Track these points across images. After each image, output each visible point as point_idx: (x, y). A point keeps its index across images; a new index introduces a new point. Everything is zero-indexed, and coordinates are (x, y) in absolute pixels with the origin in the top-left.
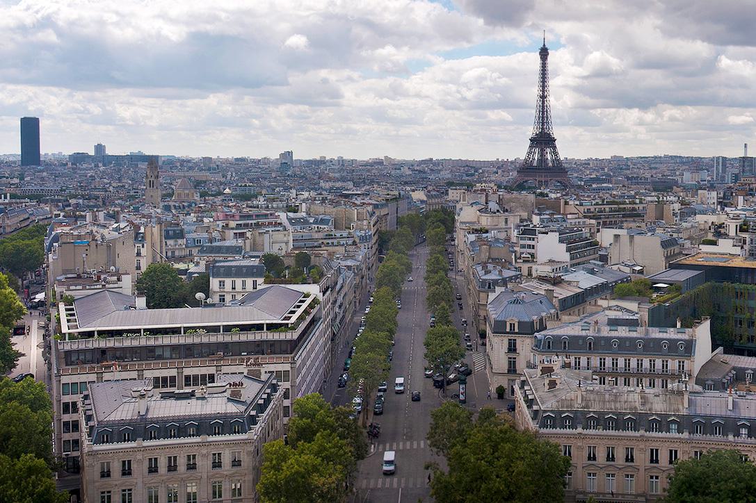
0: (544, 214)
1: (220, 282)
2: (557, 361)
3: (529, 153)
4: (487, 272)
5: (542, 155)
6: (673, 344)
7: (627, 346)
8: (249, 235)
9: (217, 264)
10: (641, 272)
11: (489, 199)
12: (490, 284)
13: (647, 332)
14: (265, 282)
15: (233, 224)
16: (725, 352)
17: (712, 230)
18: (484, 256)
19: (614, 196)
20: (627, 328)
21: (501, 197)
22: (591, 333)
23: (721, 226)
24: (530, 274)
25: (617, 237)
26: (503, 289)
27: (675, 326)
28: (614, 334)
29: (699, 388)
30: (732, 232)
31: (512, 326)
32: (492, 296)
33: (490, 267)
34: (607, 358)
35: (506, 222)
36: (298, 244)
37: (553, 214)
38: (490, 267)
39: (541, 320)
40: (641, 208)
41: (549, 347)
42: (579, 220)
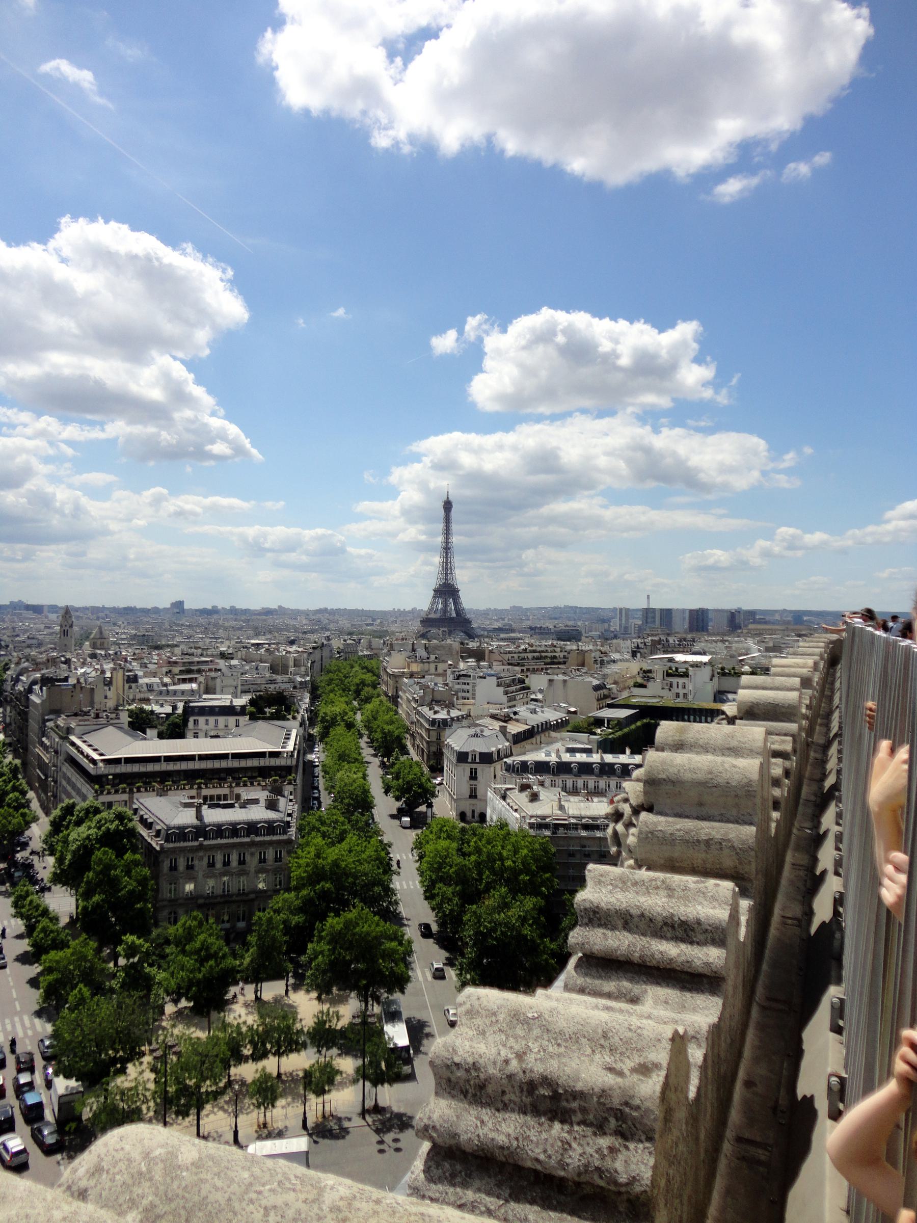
2: (532, 778)
3: (432, 604)
4: (435, 713)
5: (446, 605)
7: (585, 769)
9: (191, 704)
13: (602, 758)
14: (250, 719)
15: (176, 670)
18: (428, 699)
20: (584, 755)
22: (553, 758)
23: (650, 671)
25: (551, 681)
27: (624, 753)
31: (474, 757)
35: (436, 669)
38: (436, 708)
40: (562, 656)
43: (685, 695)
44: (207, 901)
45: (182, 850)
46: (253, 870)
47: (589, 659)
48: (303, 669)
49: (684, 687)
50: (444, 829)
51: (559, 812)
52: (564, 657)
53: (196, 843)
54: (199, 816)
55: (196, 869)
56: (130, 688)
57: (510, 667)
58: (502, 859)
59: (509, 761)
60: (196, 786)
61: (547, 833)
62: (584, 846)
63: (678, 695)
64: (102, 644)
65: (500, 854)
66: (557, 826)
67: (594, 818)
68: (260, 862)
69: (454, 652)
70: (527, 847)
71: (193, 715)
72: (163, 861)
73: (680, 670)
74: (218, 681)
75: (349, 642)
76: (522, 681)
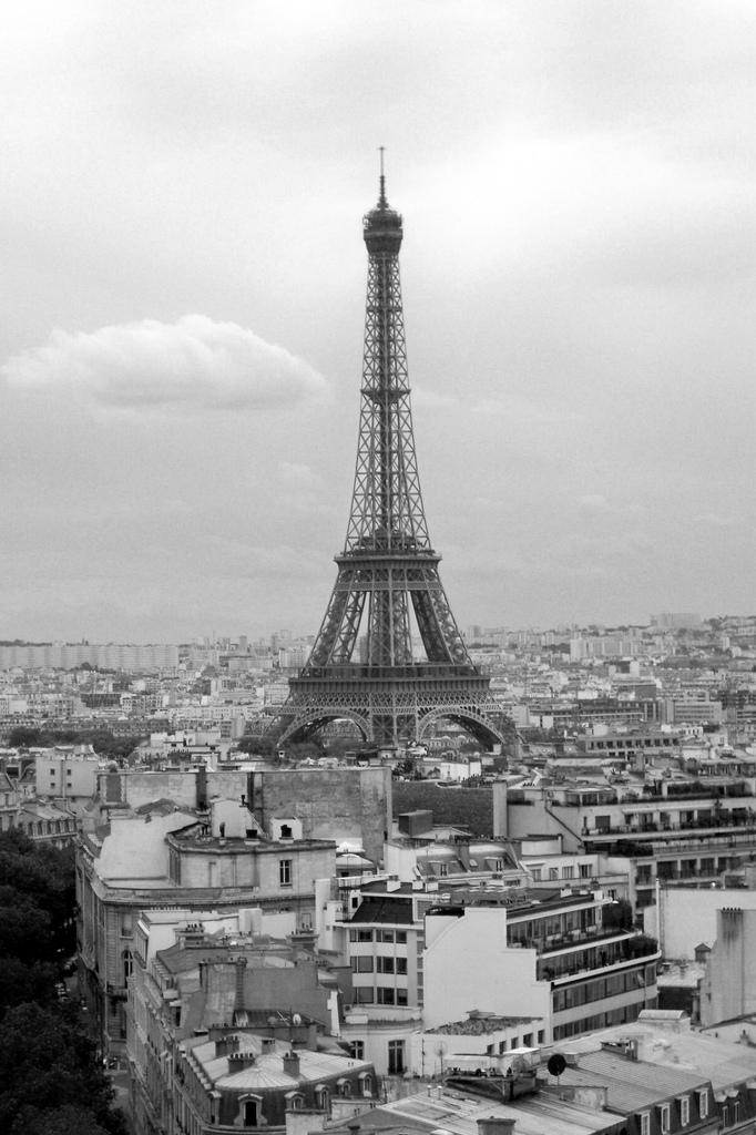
0: (426, 842)
3: (336, 613)
4: (239, 1064)
5: (385, 618)
11: (212, 788)
12: (251, 1107)
18: (221, 1005)
21: (258, 780)
25: (731, 917)
33: (249, 1044)
35: (286, 876)
57: (591, 859)
69: (370, 806)
76: (619, 917)
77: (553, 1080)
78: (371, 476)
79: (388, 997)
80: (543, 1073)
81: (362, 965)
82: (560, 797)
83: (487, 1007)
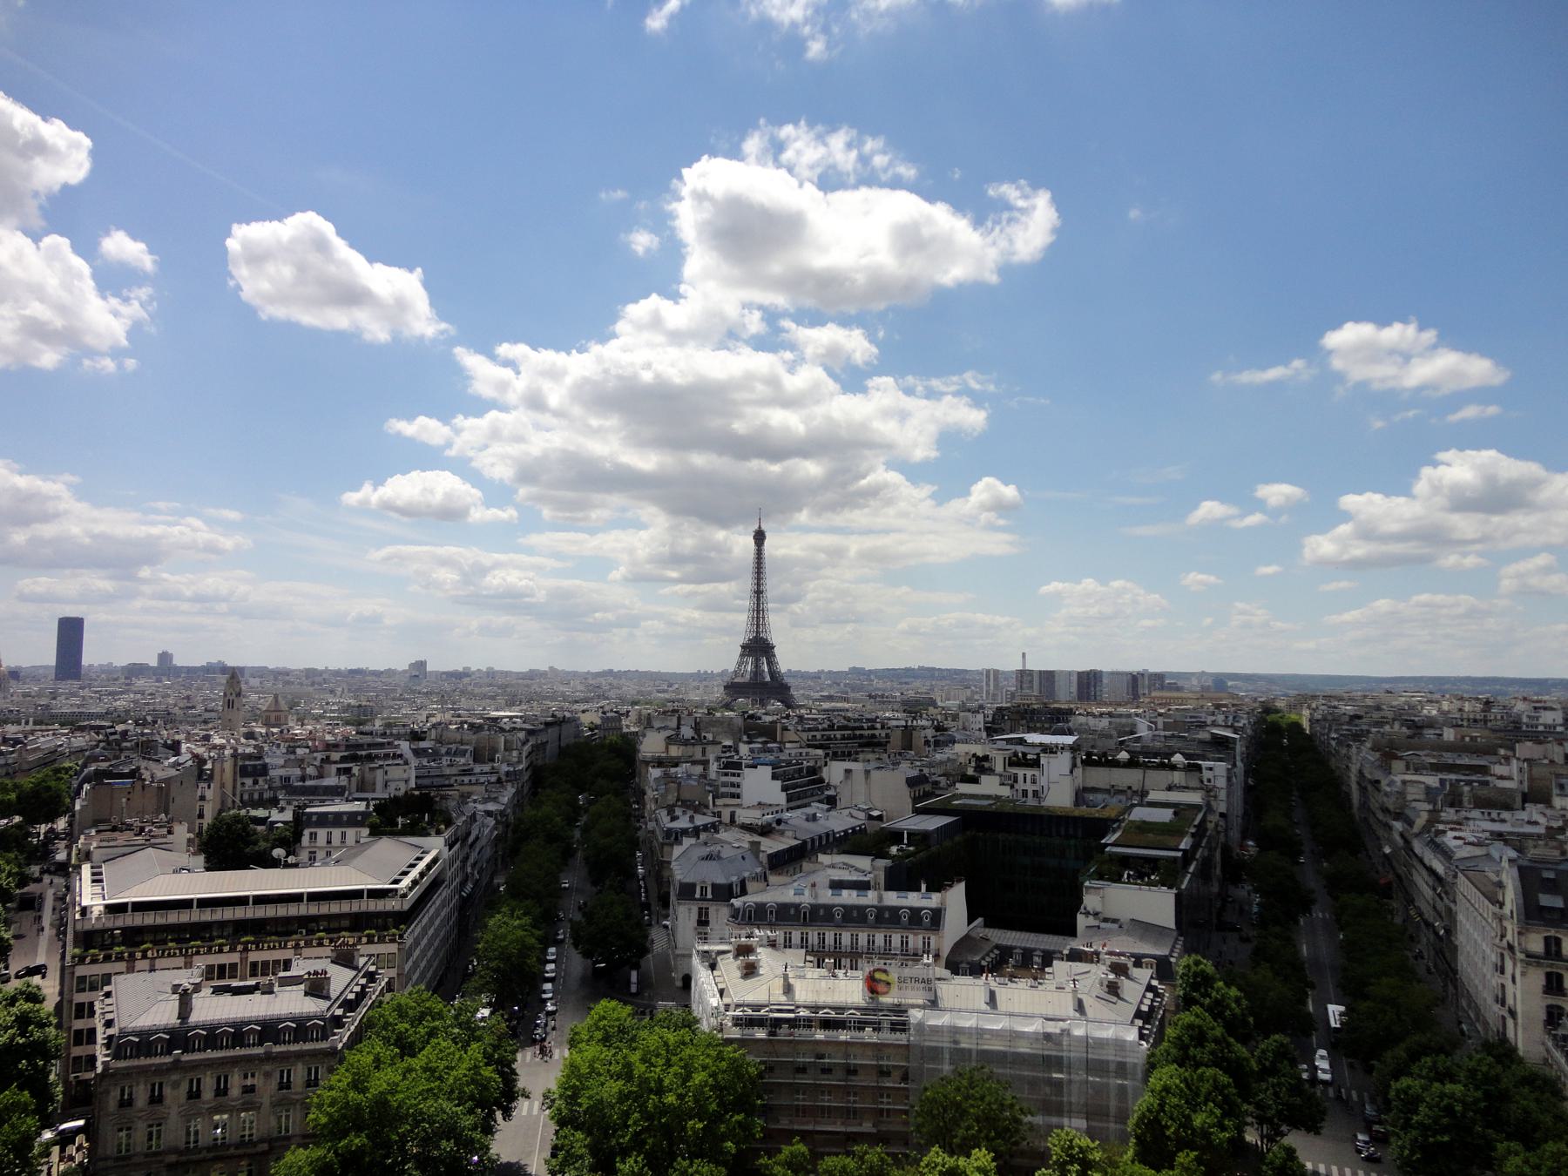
1: (311, 834)
3: (740, 664)
4: (674, 819)
5: (757, 665)
6: (915, 912)
7: (854, 917)
8: (356, 770)
9: (308, 810)
10: (880, 818)
11: (682, 722)
12: (677, 834)
13: (880, 898)
14: (371, 834)
15: (336, 756)
16: (987, 925)
17: (973, 764)
18: (671, 799)
19: (849, 720)
20: (854, 893)
22: (806, 899)
23: (986, 758)
24: (733, 821)
25: (848, 772)
26: (693, 841)
27: (919, 890)
28: (837, 900)
29: (946, 973)
30: (999, 768)
32: (677, 851)
33: (678, 812)
34: (827, 934)
35: (704, 753)
36: (419, 782)
37: (766, 742)
39: (743, 883)
40: (883, 735)
41: (750, 918)
42: (800, 750)
43: (1035, 793)
44: (184, 1158)
45: (143, 1071)
46: (266, 1101)
47: (918, 739)
48: (515, 753)
49: (1034, 782)
50: (601, 1024)
51: (783, 999)
52: (887, 736)
53: (168, 1059)
54: (185, 1009)
55: (168, 1101)
56: (255, 782)
57: (810, 750)
58: (660, 1091)
59: (737, 902)
60: (240, 948)
61: (761, 1034)
62: (822, 1056)
63: (1025, 793)
64: (278, 718)
65: (660, 1081)
66: (777, 1023)
67: (840, 1009)
68: (281, 1088)
70: (705, 1068)
71: (309, 826)
72: (107, 1092)
73: (1029, 757)
74: (379, 773)
75: (609, 714)
76: (813, 771)
77: (777, 828)
78: (753, 618)
79: (733, 796)
80: (774, 825)
81: (725, 785)
82: (800, 728)
83: (763, 801)
